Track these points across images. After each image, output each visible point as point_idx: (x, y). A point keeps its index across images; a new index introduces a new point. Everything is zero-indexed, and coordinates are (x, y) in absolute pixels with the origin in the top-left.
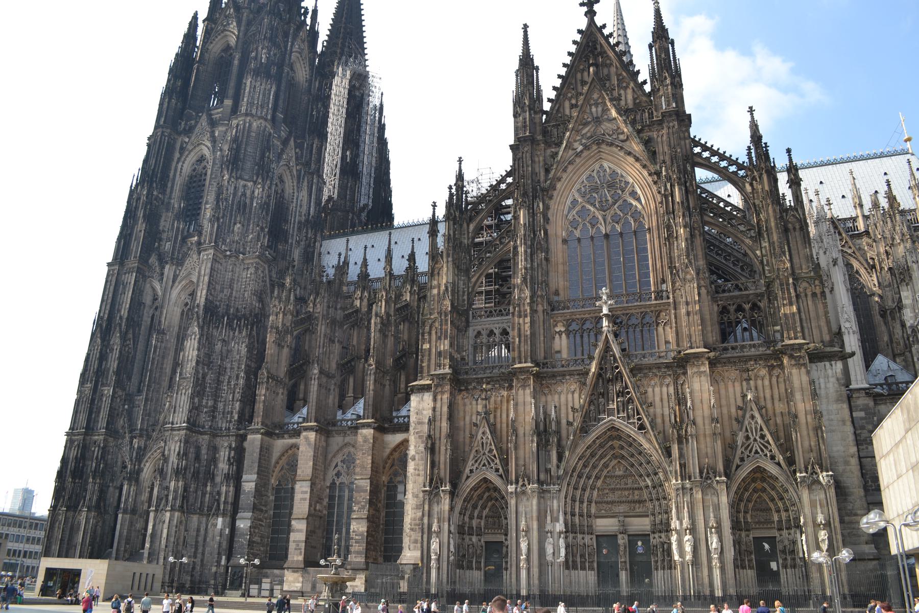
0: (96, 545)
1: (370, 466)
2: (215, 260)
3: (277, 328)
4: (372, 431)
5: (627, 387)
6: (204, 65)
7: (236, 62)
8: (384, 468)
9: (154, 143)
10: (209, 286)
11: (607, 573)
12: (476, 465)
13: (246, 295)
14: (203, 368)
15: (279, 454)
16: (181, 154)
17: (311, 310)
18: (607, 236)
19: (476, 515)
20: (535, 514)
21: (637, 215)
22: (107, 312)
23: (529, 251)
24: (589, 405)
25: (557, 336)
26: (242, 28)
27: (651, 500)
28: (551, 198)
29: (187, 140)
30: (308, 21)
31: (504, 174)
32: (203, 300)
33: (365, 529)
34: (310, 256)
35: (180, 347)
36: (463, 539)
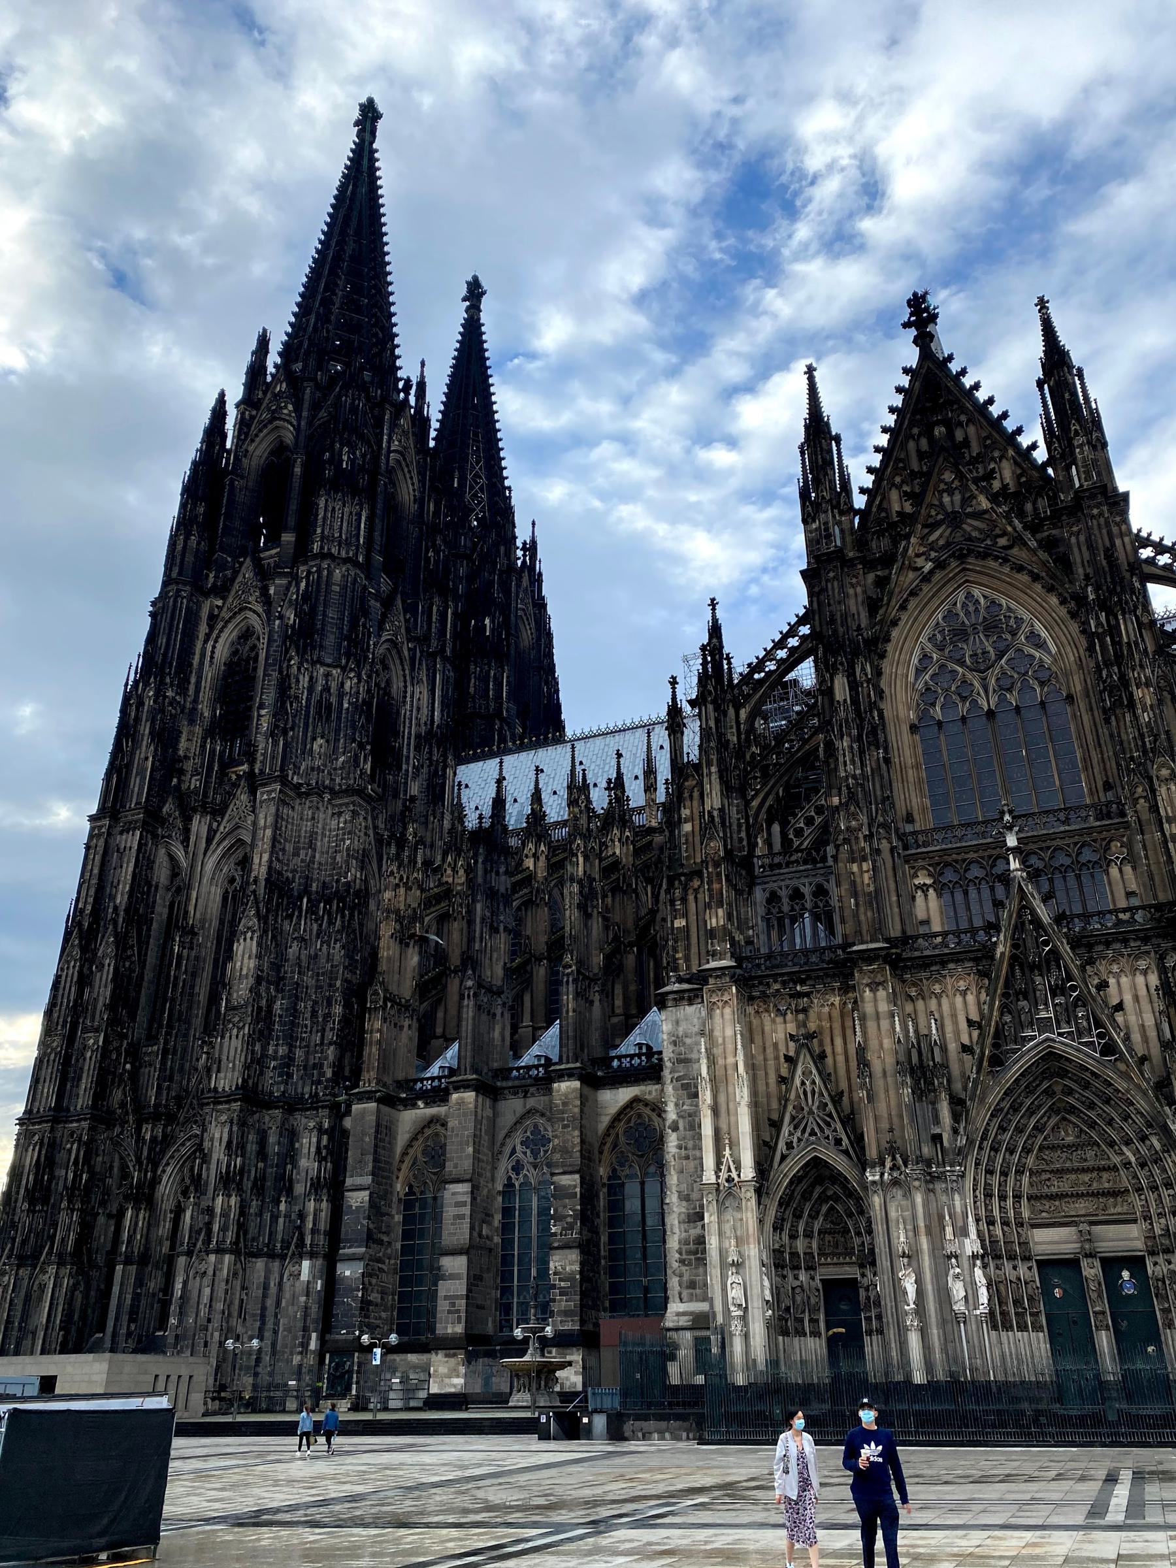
0: (73, 1329)
1: (578, 1148)
3: (397, 912)
4: (577, 1084)
5: (1070, 977)
6: (242, 477)
7: (298, 470)
8: (601, 1153)
9: (160, 611)
10: (273, 846)
11: (1070, 1335)
12: (799, 1134)
13: (338, 859)
14: (268, 989)
15: (407, 1137)
16: (211, 628)
17: (450, 880)
18: (990, 714)
19: (801, 1229)
20: (921, 1224)
22: (91, 900)
23: (855, 746)
24: (1002, 1014)
25: (919, 893)
26: (305, 414)
27: (1139, 1190)
28: (882, 656)
29: (220, 603)
30: (412, 400)
31: (794, 620)
32: (264, 870)
33: (577, 1268)
34: (439, 791)
35: (225, 953)
36: (784, 1277)
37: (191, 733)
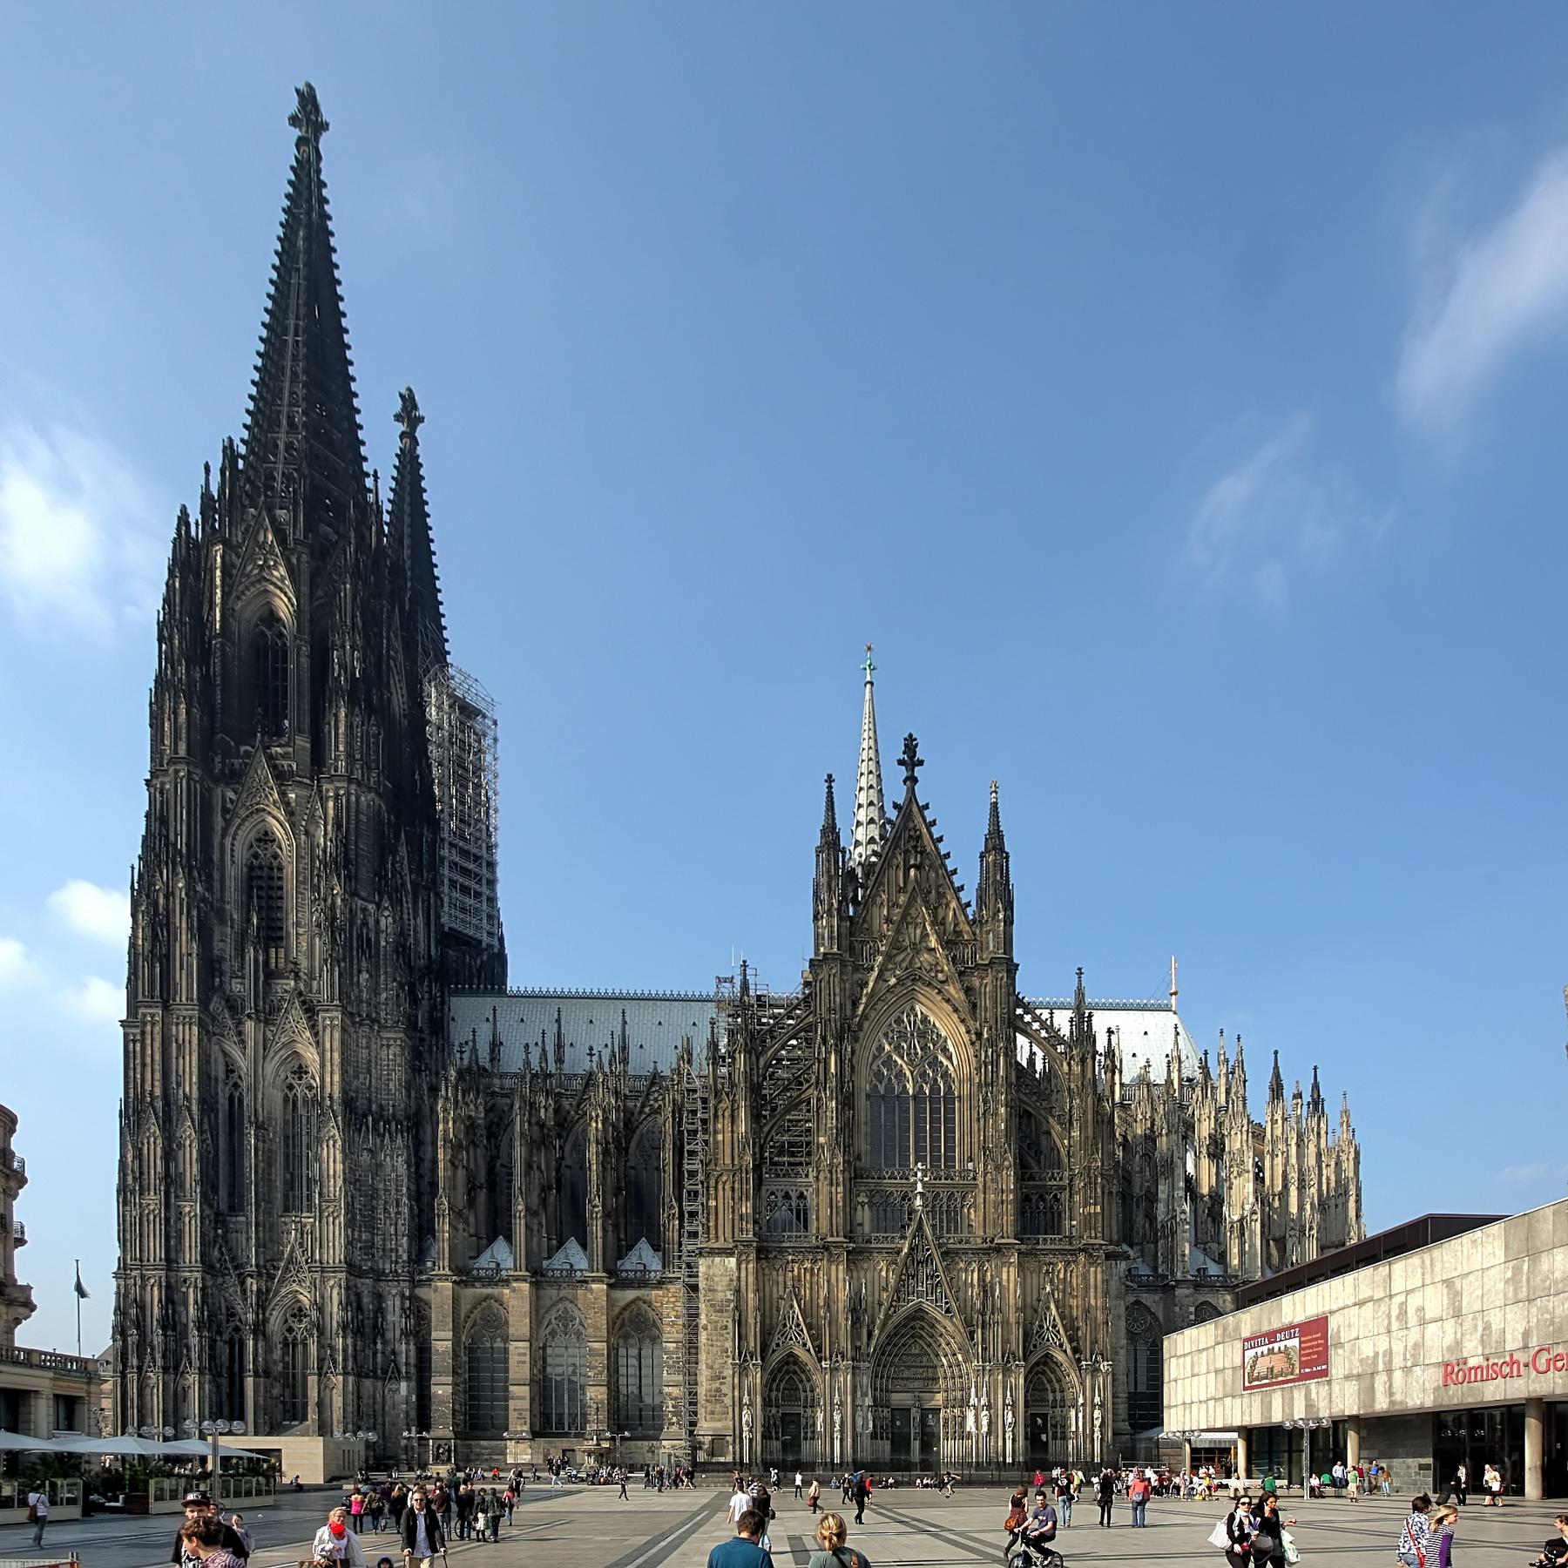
2: (344, 1030)
21: (945, 1075)
37: (223, 933)
